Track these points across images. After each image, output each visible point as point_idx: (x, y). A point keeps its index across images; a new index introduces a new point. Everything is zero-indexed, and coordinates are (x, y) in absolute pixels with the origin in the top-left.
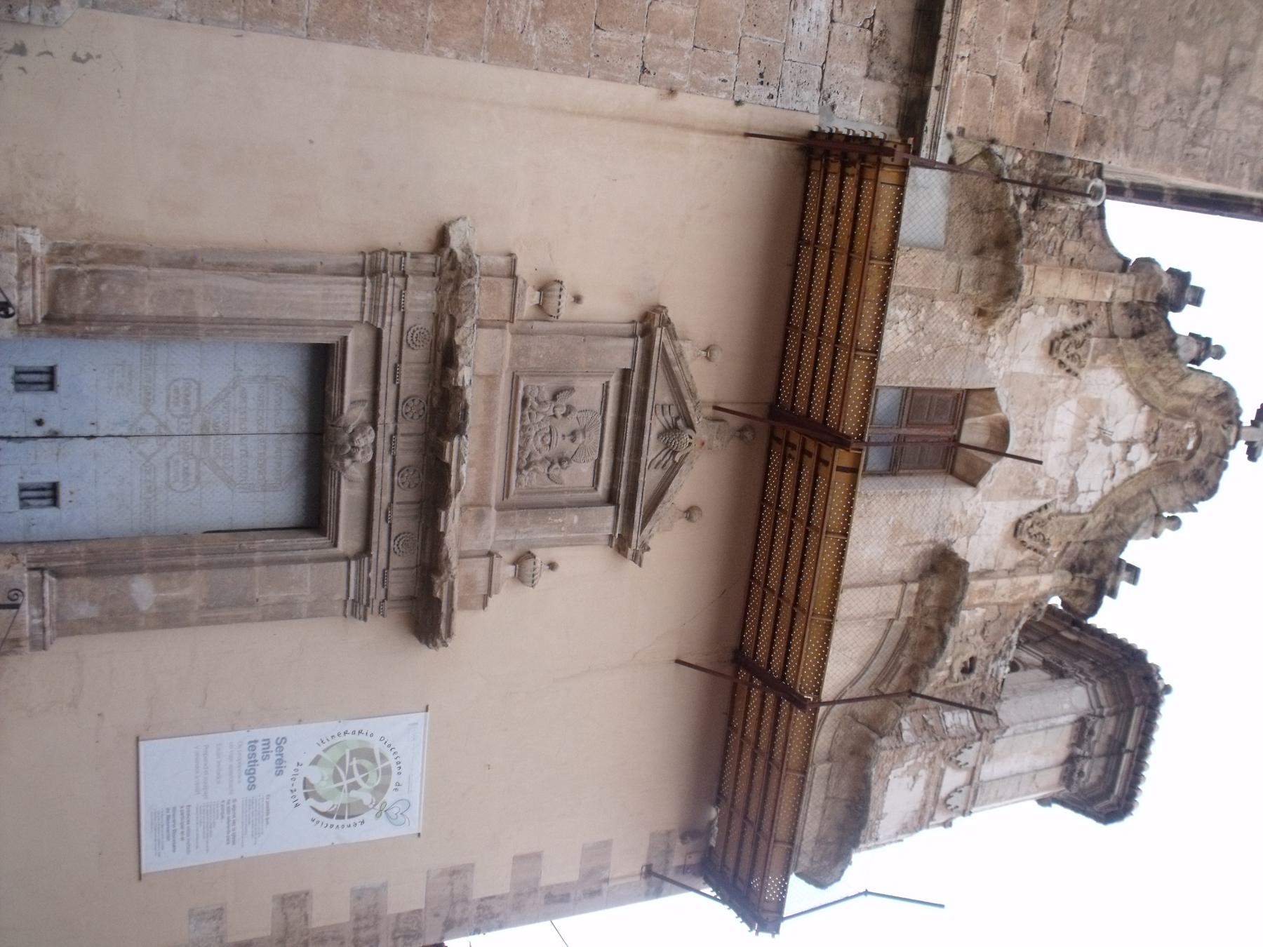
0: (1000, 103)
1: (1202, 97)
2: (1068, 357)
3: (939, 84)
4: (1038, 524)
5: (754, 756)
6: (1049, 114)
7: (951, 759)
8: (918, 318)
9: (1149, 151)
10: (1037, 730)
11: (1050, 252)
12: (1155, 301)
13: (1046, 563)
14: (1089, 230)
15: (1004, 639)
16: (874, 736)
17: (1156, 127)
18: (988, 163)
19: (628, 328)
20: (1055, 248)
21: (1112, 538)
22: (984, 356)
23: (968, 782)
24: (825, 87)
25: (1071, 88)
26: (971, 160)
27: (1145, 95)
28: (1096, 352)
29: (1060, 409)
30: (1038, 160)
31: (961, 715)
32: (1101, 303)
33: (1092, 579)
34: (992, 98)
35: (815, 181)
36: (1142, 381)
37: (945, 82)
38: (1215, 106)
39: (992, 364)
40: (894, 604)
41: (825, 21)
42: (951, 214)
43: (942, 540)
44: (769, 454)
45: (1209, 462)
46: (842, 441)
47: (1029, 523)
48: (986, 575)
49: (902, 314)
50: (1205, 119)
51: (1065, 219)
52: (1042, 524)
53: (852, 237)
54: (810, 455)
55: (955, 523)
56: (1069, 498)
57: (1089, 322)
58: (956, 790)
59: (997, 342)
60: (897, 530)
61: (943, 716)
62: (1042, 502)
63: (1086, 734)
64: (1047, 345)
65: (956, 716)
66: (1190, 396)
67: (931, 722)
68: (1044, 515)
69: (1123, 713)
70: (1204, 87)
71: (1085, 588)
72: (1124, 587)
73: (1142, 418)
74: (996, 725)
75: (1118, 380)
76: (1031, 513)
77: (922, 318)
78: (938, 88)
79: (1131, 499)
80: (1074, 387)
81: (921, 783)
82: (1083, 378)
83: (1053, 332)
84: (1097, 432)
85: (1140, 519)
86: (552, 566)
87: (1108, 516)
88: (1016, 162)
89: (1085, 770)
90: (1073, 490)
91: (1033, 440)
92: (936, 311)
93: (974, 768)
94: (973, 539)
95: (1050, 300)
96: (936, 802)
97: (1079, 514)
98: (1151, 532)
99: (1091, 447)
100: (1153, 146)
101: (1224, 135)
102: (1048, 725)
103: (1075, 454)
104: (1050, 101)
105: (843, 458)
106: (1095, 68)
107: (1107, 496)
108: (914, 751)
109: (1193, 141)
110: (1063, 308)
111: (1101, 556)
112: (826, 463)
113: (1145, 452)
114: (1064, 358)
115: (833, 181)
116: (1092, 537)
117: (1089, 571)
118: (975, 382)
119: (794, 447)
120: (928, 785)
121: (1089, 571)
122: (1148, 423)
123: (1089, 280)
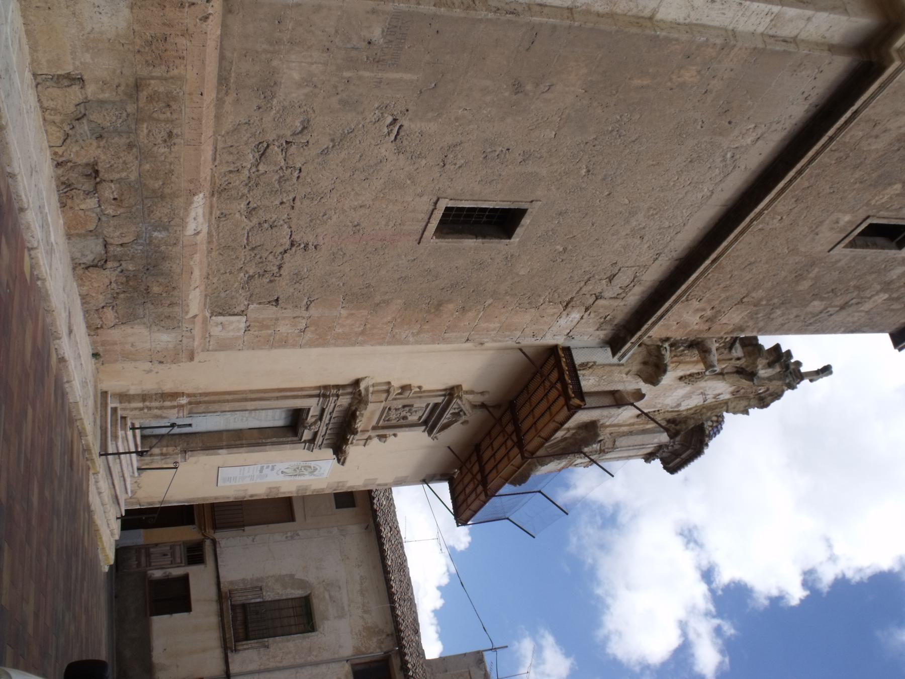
6: (710, 328)
16: (537, 464)
19: (443, 393)
21: (693, 418)
41: (576, 320)
45: (771, 395)
78: (632, 343)
86: (395, 435)
117: (676, 425)
121: (676, 425)
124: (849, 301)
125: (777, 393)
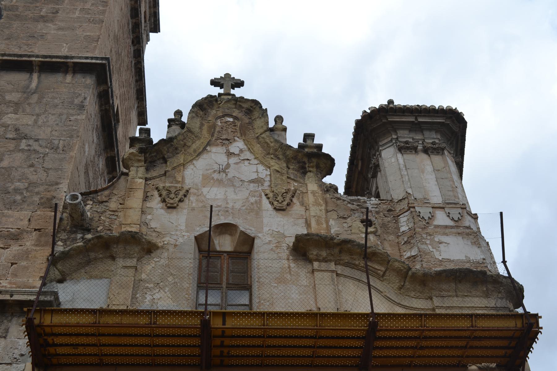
0: (27, 258)
1: (32, 148)
2: (177, 197)
3: (9, 295)
4: (276, 198)
5: (422, 348)
6: (35, 230)
7: (428, 223)
8: (152, 288)
9: (60, 172)
10: (408, 174)
11: (115, 217)
12: (143, 155)
13: (301, 189)
14: (104, 197)
15: (349, 205)
16: (410, 273)
17: (46, 170)
18: (59, 261)
20: (113, 215)
21: (284, 154)
22: (176, 246)
23: (443, 209)
24: (10, 362)
25: (22, 220)
26: (58, 270)
27: (28, 179)
28: (174, 182)
29: (208, 197)
30: (62, 231)
31: (402, 222)
32: (145, 184)
33: (308, 161)
35: (64, 360)
36: (193, 153)
37: (8, 292)
38: (37, 140)
39: (181, 240)
40: (327, 275)
42: (91, 277)
43: (287, 252)
44: (232, 366)
46: (205, 324)
47: (275, 203)
48: (309, 222)
49: (149, 297)
50: (44, 144)
51: (97, 211)
52: (276, 196)
53: (87, 335)
54: (222, 342)
55: (277, 247)
56: (261, 183)
57: (157, 188)
58: (448, 216)
59: (167, 239)
60: (281, 280)
61: (402, 232)
62: (264, 197)
63: (407, 145)
64: (170, 210)
65: (401, 225)
66: (202, 125)
67: (406, 240)
68: (271, 195)
69: (395, 127)
70: (26, 148)
71: (315, 163)
72: (316, 141)
73: (214, 149)
74: (406, 199)
75: (192, 167)
76: (270, 203)
77: (152, 285)
78: (11, 296)
79: (263, 147)
80: (196, 191)
81: (444, 239)
82: (190, 186)
83: (162, 208)
84: (222, 173)
85: (272, 140)
87: (272, 158)
88: (62, 244)
89: (431, 141)
90: (258, 181)
91: (226, 210)
92: (148, 278)
93: (433, 208)
94: (286, 234)
95: (143, 212)
96: (457, 227)
97: (270, 175)
98: (283, 133)
99: (230, 176)
100: (56, 170)
101: (54, 133)
102: (404, 169)
103: (235, 184)
104: (27, 230)
105: (217, 323)
106: (11, 209)
107: (261, 161)
108: (423, 247)
109: (55, 149)
110: (148, 204)
111: (295, 158)
112: (223, 332)
113: (235, 144)
114: (177, 199)
115: (60, 350)
116: (285, 165)
118: (192, 246)
119: (222, 352)
120: (446, 234)
122: (217, 145)
123: (132, 193)
124: (10, 138)
125: (236, 104)
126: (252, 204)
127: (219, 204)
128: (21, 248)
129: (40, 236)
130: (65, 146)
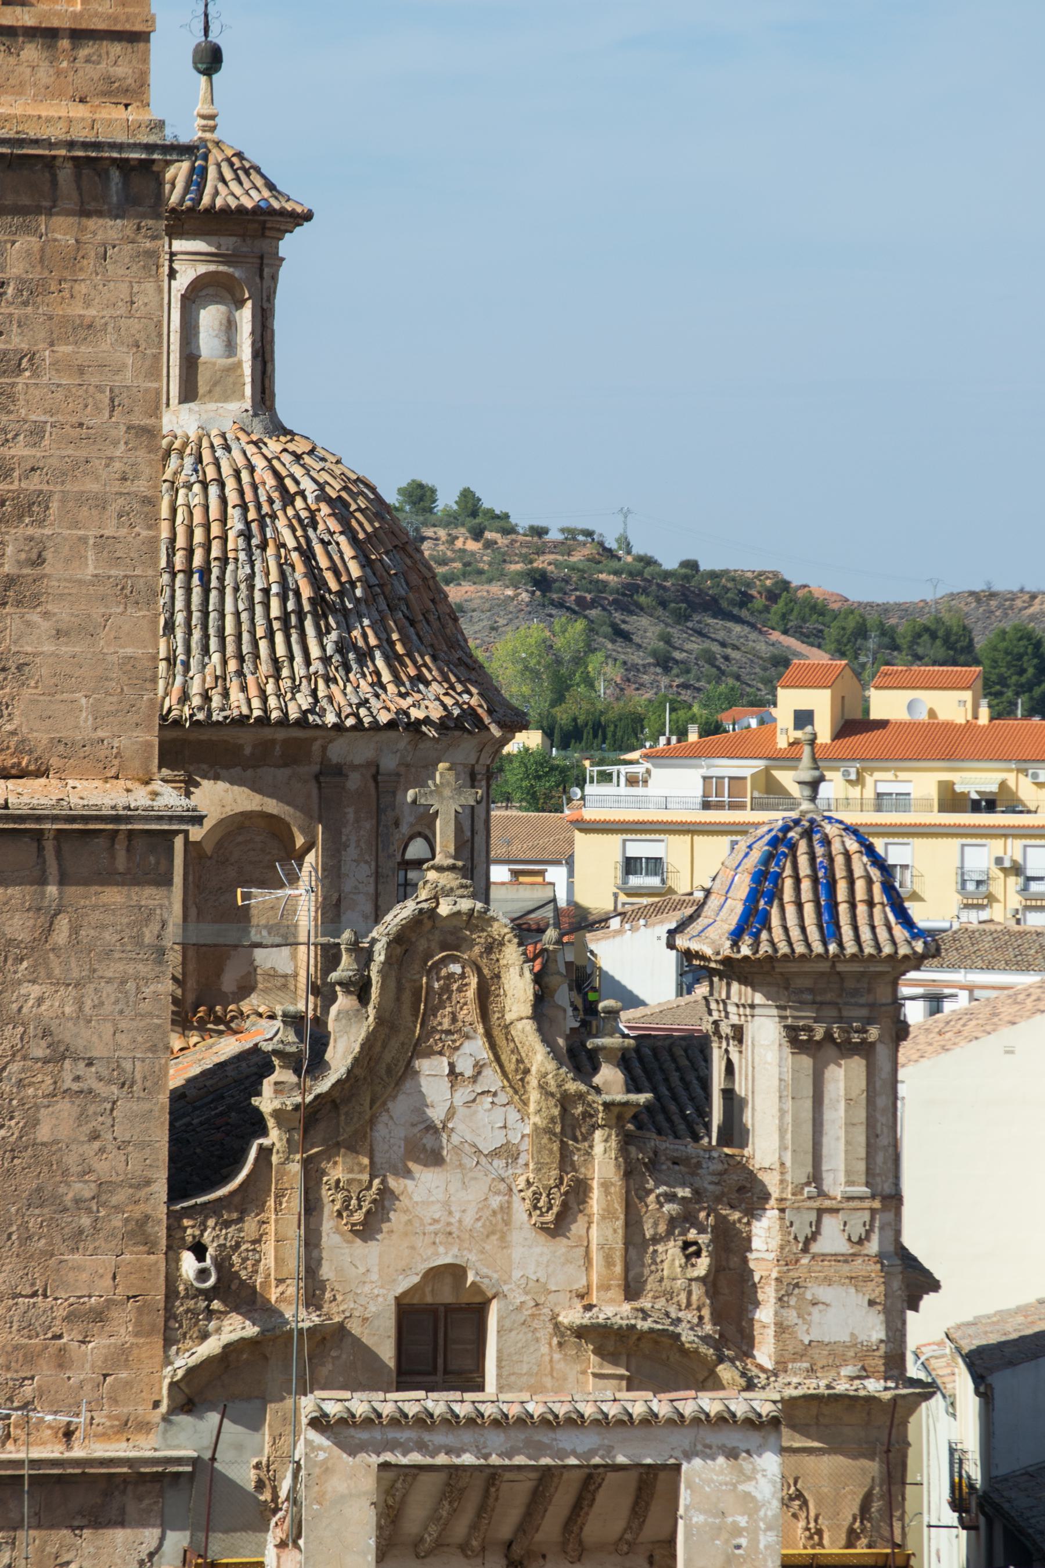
22: (365, 1320)
34: (124, 1375)
39: (372, 1308)
126: (494, 1213)
127: (437, 1216)
128: (113, 1340)
129: (140, 1311)
130: (145, 1077)
